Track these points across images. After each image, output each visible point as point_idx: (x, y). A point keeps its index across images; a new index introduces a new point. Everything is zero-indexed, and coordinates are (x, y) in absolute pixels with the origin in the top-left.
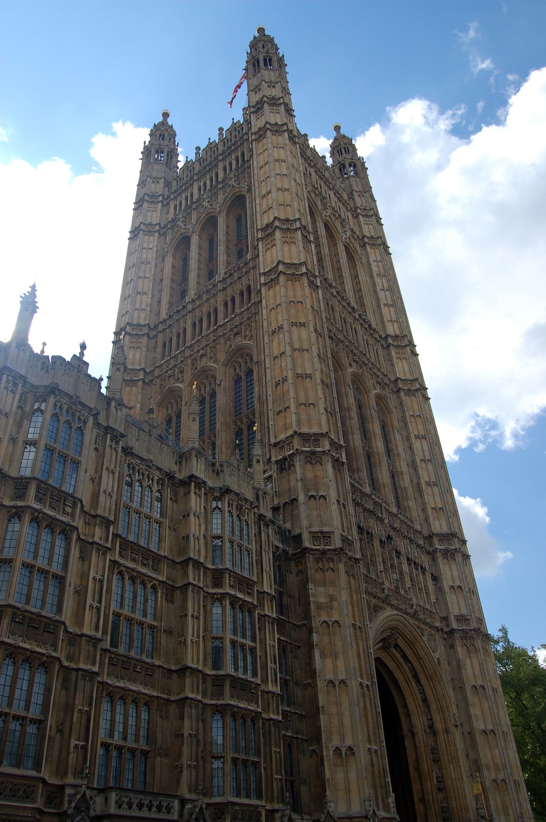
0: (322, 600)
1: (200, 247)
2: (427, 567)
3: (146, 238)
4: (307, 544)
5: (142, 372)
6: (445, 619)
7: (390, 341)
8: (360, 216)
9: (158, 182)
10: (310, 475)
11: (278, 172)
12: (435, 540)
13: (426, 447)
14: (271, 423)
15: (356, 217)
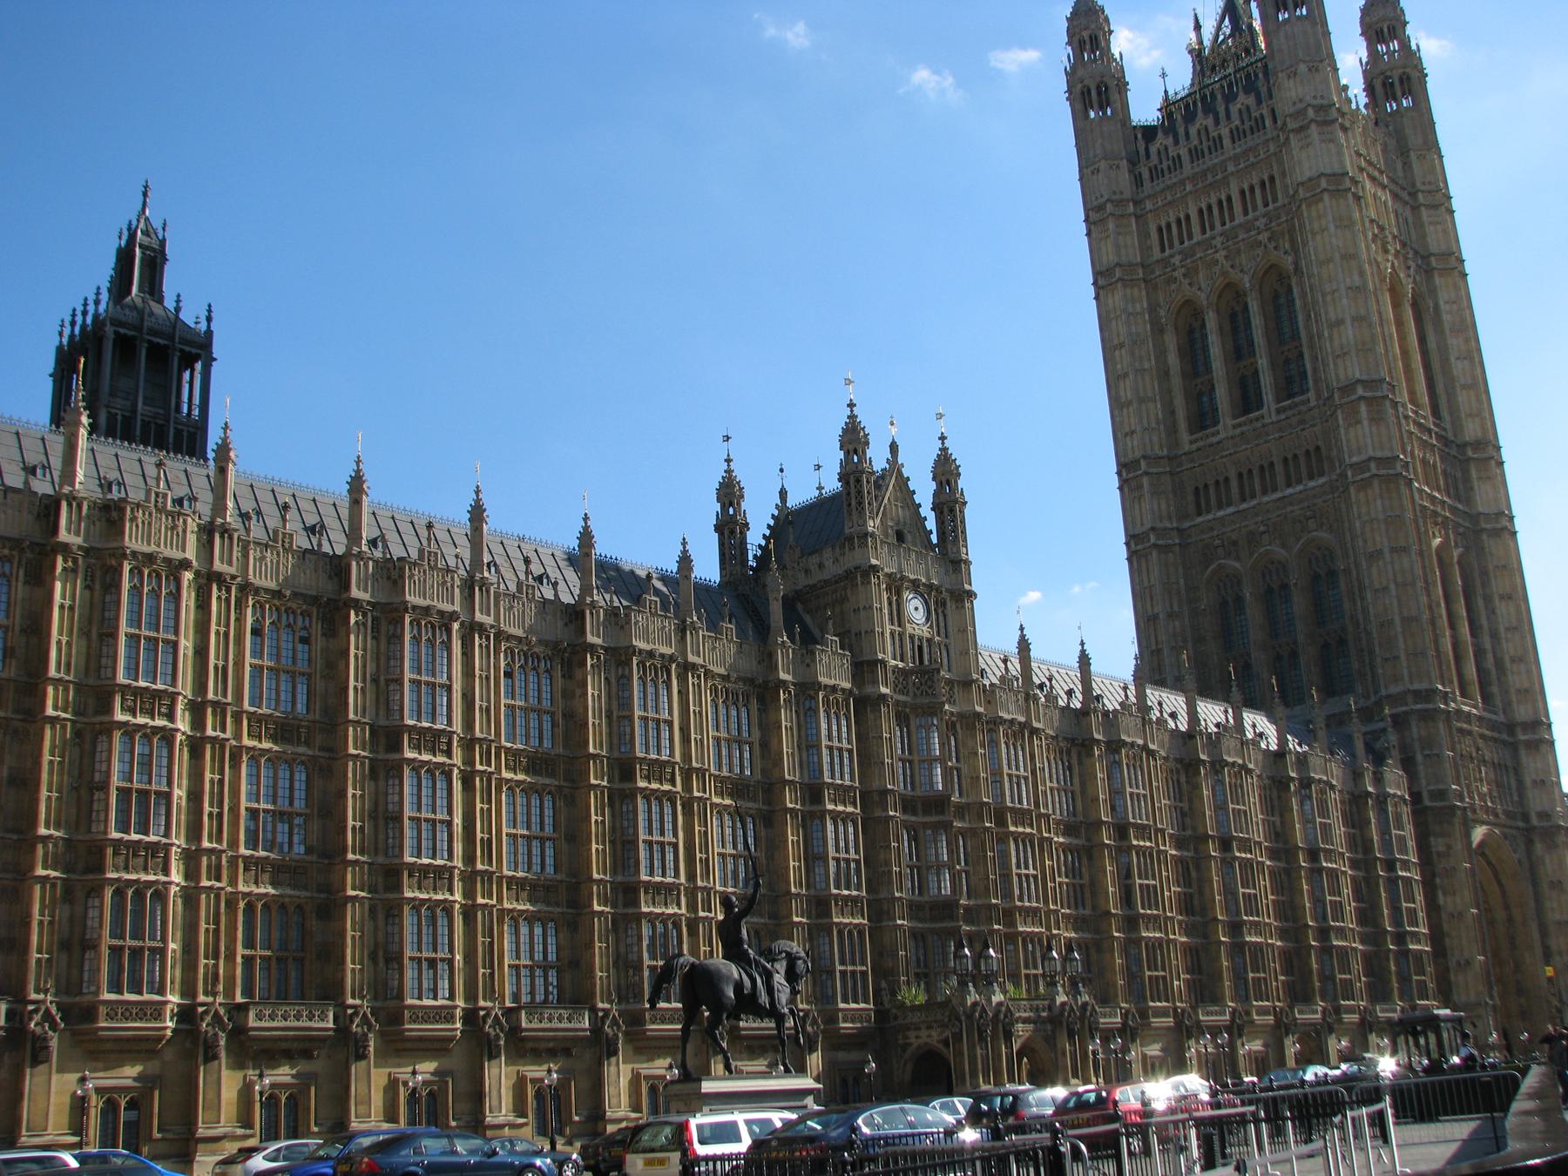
0: (1441, 849)
1: (1221, 328)
2: (1509, 763)
3: (1128, 291)
4: (1427, 802)
5: (1175, 532)
6: (1526, 817)
7: (1470, 453)
8: (1423, 209)
9: (1118, 167)
10: (1423, 733)
11: (1348, 283)
12: (1519, 730)
13: (1512, 610)
14: (1380, 671)
15: (1415, 209)
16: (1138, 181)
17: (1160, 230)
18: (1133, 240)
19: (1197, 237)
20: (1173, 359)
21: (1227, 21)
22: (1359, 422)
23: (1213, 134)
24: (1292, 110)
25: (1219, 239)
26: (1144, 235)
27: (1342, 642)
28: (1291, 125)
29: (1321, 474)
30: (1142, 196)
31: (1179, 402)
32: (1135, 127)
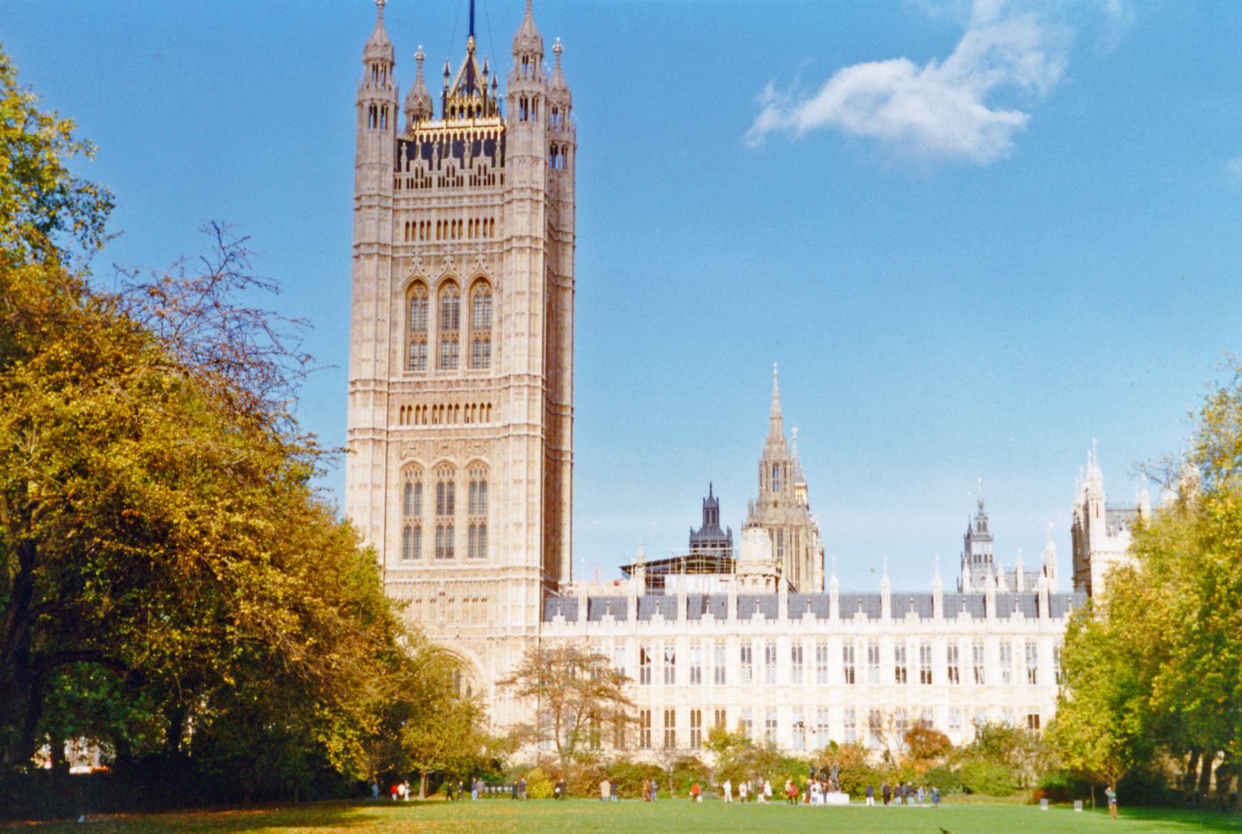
16: (397, 184)
17: (407, 225)
18: (389, 227)
19: (433, 240)
20: (401, 317)
21: (465, 75)
22: (521, 399)
23: (459, 172)
24: (519, 186)
25: (449, 249)
26: (396, 224)
27: (483, 527)
28: (516, 195)
29: (488, 421)
30: (397, 196)
31: (400, 347)
32: (400, 142)
